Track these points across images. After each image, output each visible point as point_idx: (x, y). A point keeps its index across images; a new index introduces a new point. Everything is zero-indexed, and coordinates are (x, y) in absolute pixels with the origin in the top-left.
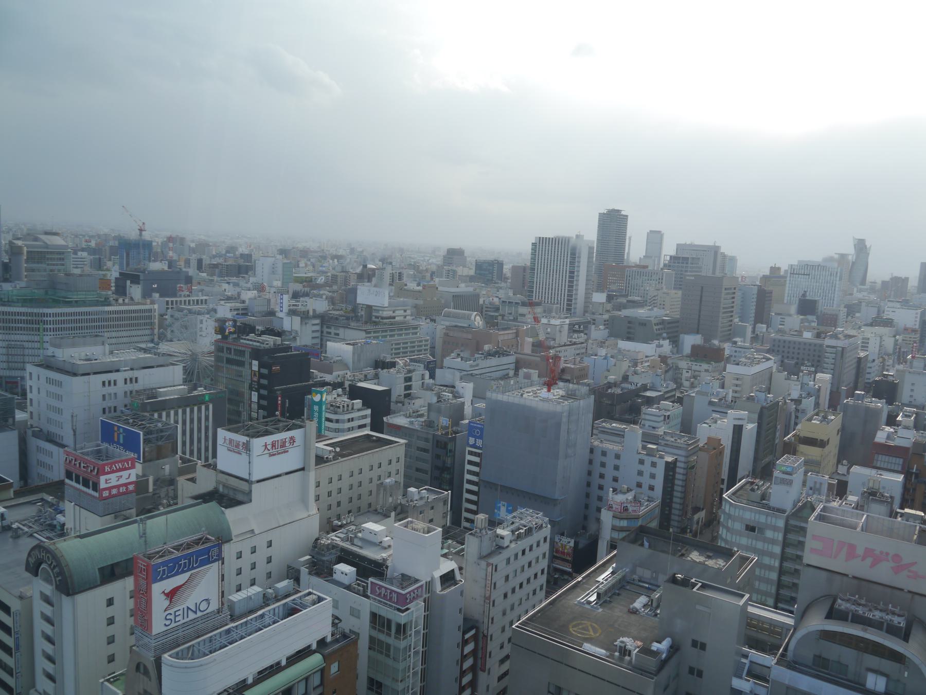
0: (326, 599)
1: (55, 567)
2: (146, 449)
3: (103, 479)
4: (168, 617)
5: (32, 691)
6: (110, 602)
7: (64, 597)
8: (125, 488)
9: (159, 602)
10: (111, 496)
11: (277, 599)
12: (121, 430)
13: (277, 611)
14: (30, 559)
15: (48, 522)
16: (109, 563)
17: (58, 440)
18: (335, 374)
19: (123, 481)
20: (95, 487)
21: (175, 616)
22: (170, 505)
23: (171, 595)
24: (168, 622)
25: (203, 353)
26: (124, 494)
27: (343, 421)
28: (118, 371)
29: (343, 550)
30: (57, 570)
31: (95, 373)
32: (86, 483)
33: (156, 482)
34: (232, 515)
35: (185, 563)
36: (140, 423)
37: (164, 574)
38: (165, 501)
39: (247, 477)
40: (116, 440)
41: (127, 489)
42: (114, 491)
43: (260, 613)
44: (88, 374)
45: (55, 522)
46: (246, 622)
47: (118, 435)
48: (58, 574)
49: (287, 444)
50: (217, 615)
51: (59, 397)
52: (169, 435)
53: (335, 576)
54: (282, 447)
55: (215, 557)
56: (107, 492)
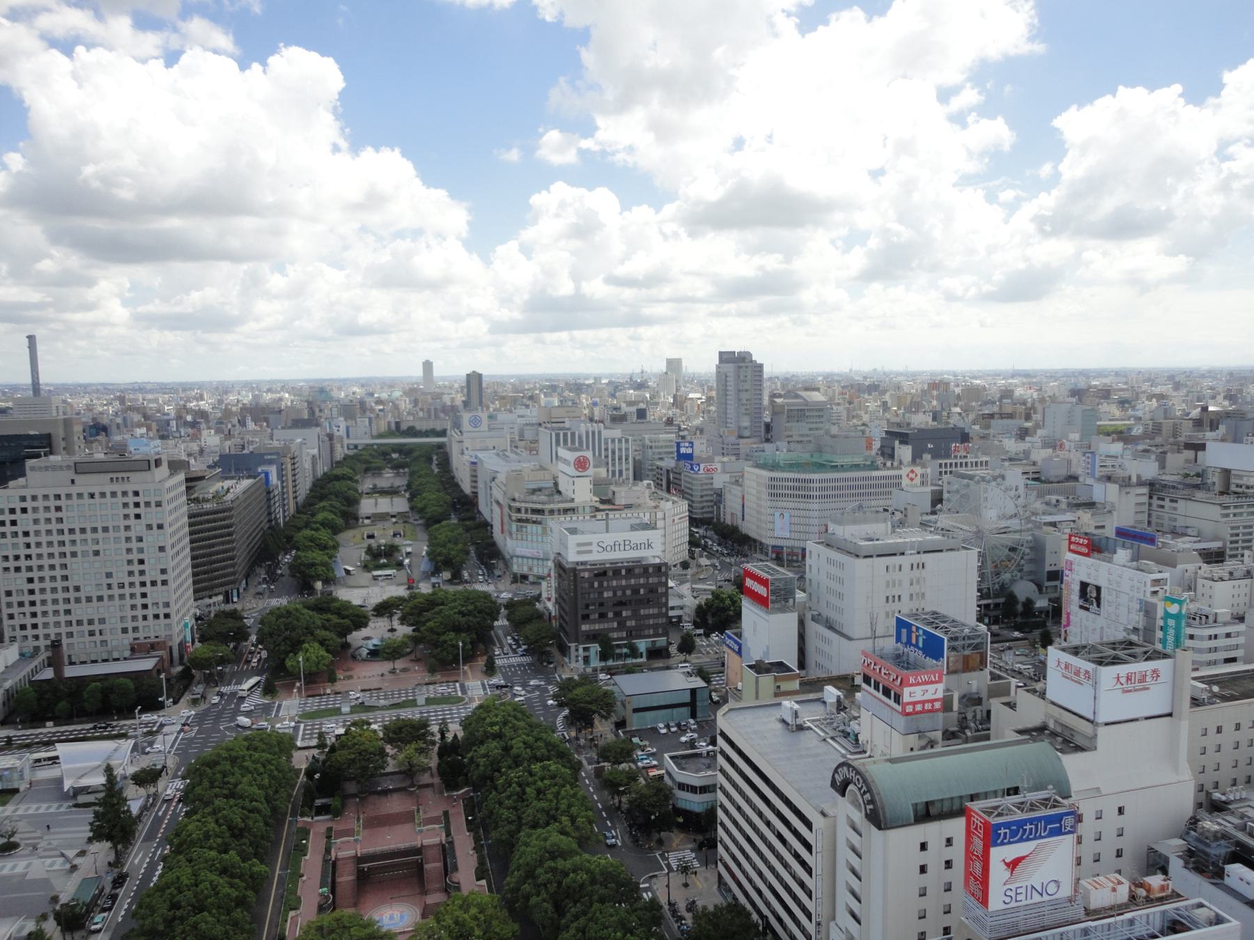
0: (1230, 921)
1: (865, 793)
2: (951, 659)
3: (907, 691)
4: (1009, 893)
5: (832, 924)
6: (923, 847)
7: (873, 829)
8: (930, 705)
9: (998, 873)
10: (915, 713)
11: (1149, 901)
12: (921, 632)
13: (1151, 917)
14: (836, 776)
15: (841, 728)
16: (925, 800)
17: (837, 628)
18: (1179, 567)
19: (928, 696)
20: (898, 699)
21: (1017, 894)
22: (979, 731)
23: (1013, 865)
24: (1008, 900)
25: (991, 532)
26: (929, 711)
27: (1201, 638)
28: (903, 554)
29: (1239, 844)
30: (868, 796)
31: (878, 556)
32: (887, 692)
33: (961, 698)
34: (1072, 764)
35: (1031, 829)
36: (942, 625)
37: (1005, 837)
38: (972, 725)
39: (1091, 717)
40: (914, 641)
41: (933, 706)
42: (919, 707)
43: (1128, 916)
44: (871, 556)
45: (848, 730)
46: (1109, 924)
47: (917, 637)
48: (872, 802)
49: (1148, 679)
50: (1069, 904)
51: (841, 581)
52: (977, 644)
53: (1227, 881)
54: (1140, 681)
55: (1068, 829)
56: (911, 707)
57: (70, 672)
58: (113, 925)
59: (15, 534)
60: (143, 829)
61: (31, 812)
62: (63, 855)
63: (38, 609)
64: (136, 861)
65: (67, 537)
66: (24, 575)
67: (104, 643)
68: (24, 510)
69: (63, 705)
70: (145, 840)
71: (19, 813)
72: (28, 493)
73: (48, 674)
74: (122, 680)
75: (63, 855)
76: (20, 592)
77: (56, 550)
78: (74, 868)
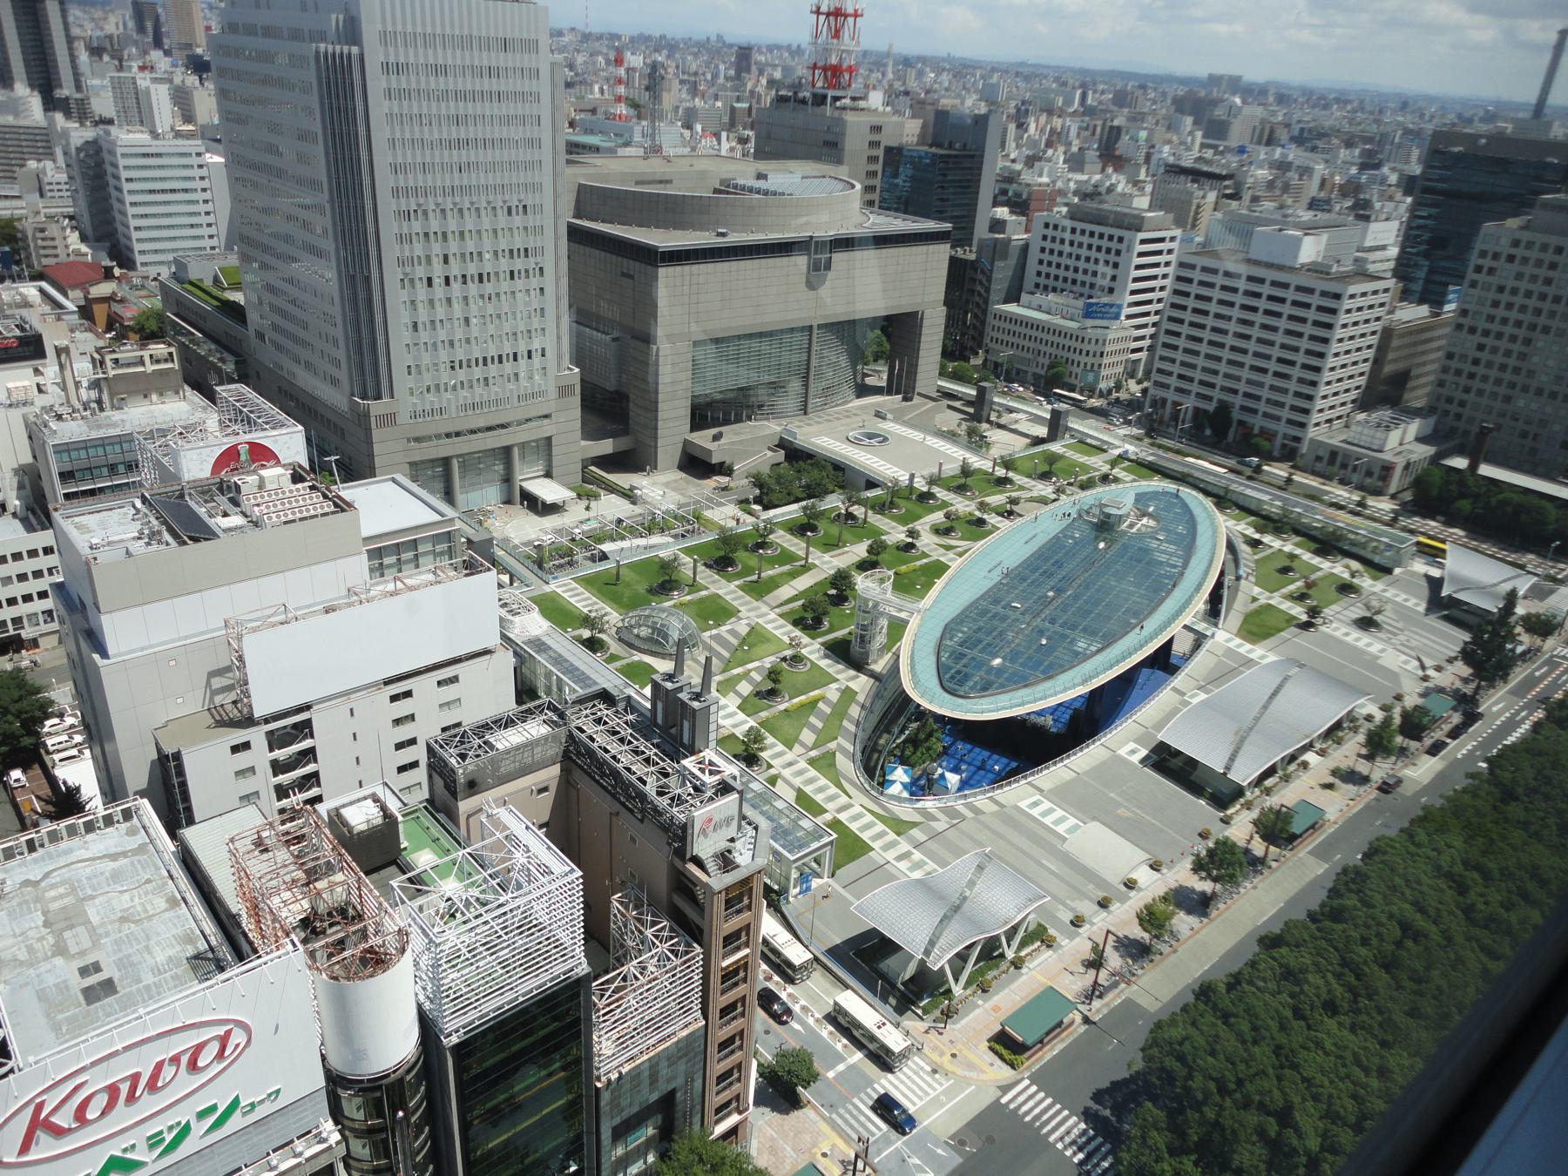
57: (1486, 470)
58: (1451, 758)
59: (1487, 287)
60: (1518, 675)
61: (1398, 599)
62: (1419, 660)
63: (1476, 384)
64: (1495, 709)
65: (1547, 306)
66: (1478, 338)
67: (1534, 451)
68: (1511, 259)
69: (1465, 505)
70: (1513, 692)
71: (1387, 595)
72: (1526, 236)
73: (1460, 463)
74: (1549, 506)
75: (1419, 660)
76: (1463, 357)
77: (1527, 318)
78: (1425, 678)
